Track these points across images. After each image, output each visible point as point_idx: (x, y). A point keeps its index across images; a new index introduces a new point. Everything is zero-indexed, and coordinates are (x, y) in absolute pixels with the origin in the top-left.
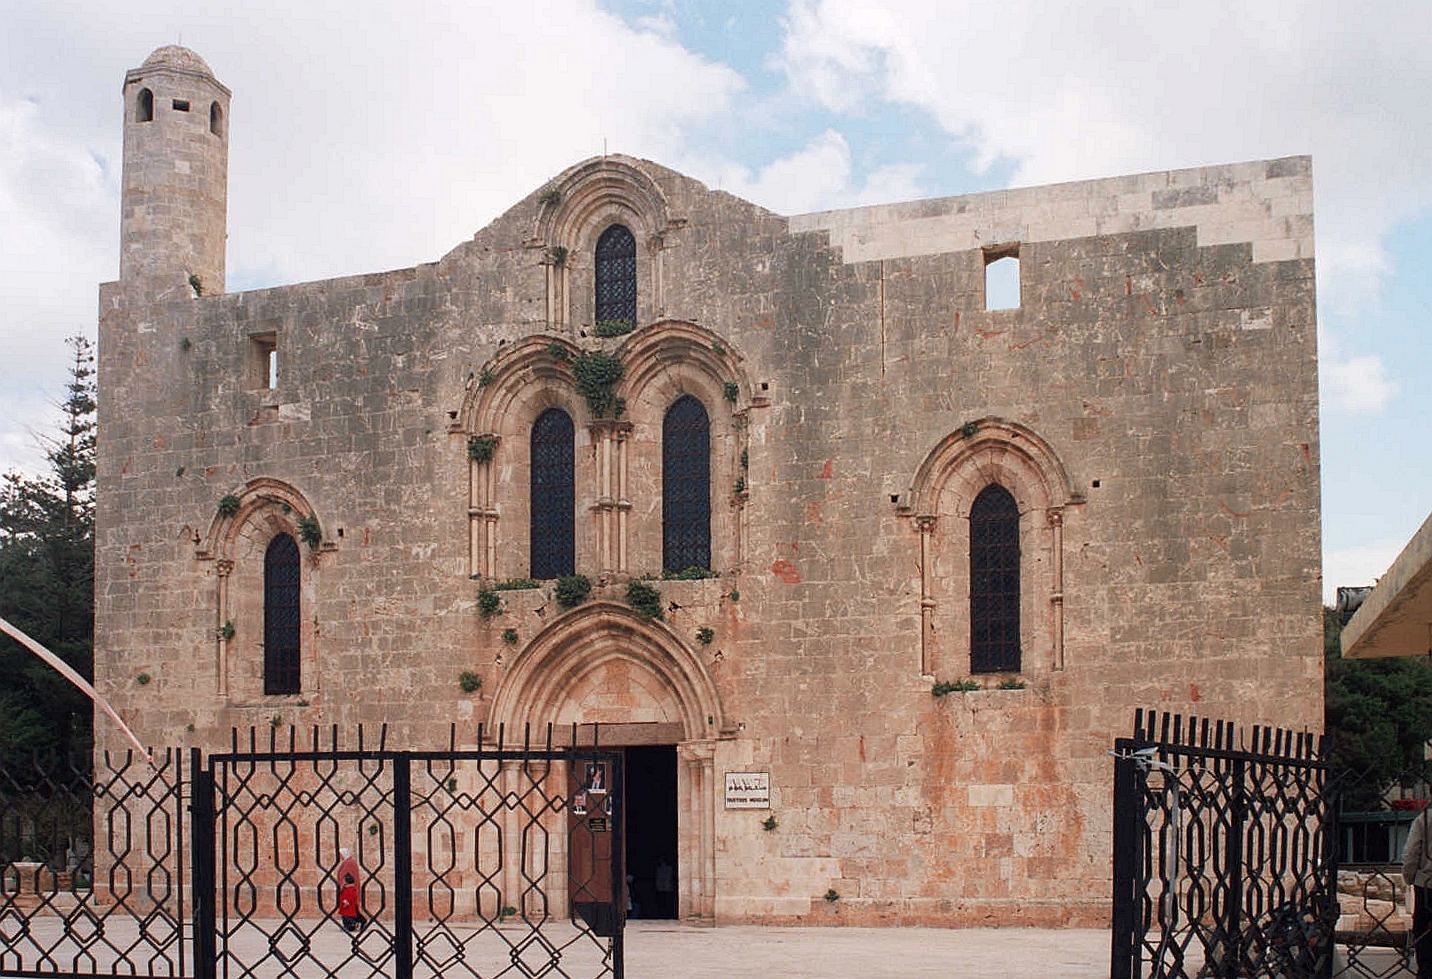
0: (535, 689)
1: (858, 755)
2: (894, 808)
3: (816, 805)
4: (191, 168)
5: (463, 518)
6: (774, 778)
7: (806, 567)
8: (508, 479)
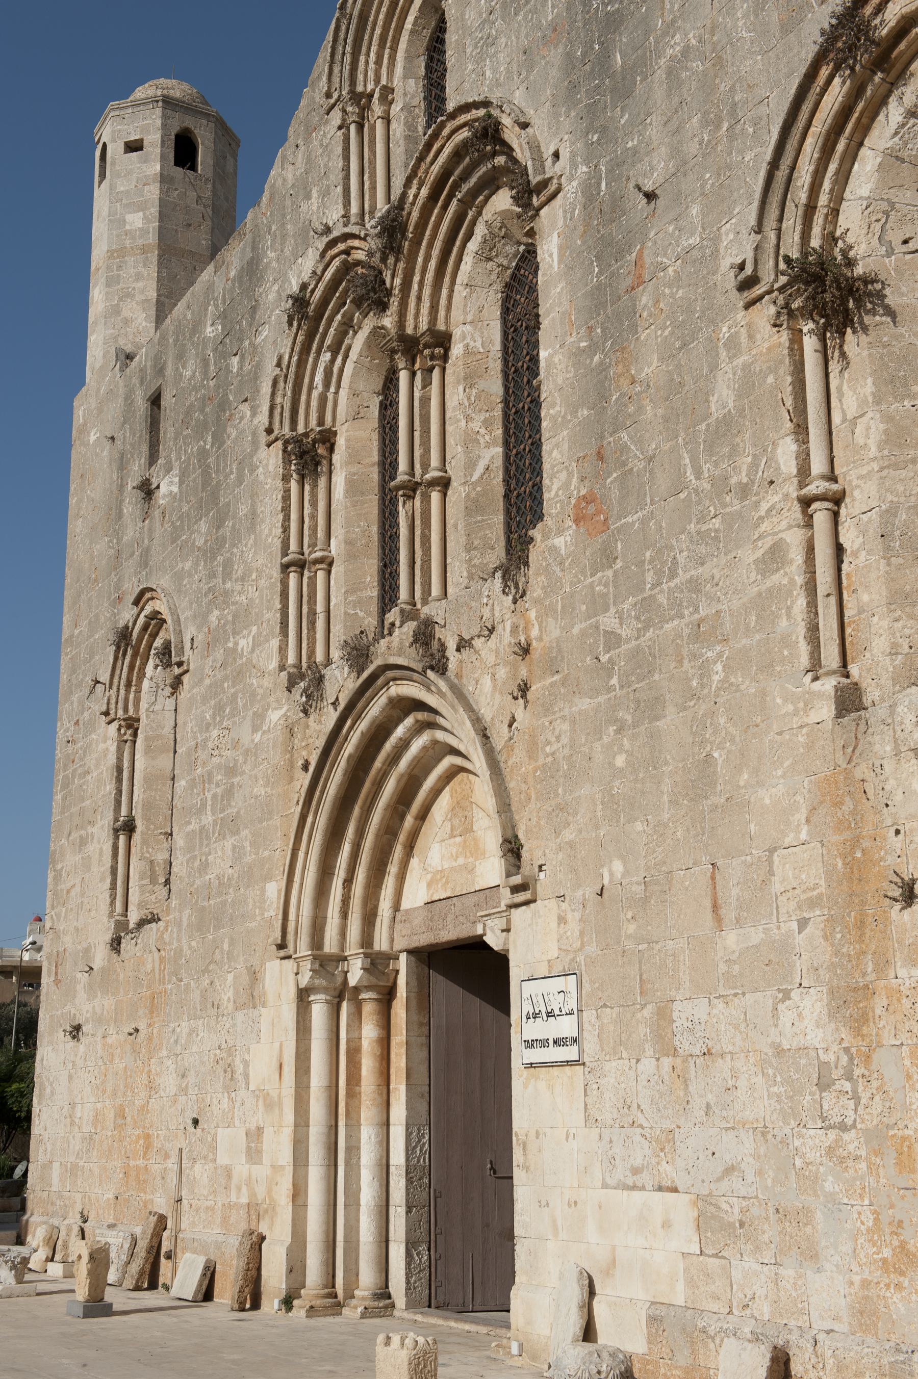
1: (709, 915)
2: (779, 1051)
3: (649, 1052)
4: (145, 217)
5: (276, 574)
6: (586, 986)
7: (615, 493)
8: (341, 495)
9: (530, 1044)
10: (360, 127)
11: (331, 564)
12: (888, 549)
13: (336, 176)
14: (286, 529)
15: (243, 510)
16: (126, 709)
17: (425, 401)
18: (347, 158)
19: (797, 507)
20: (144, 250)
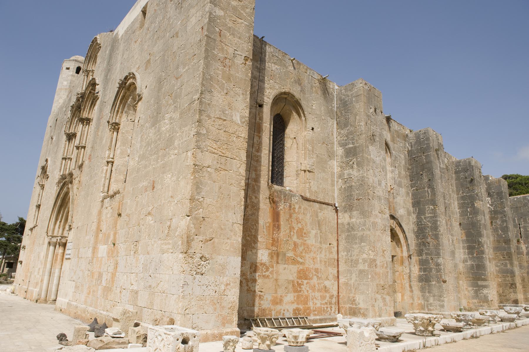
0: (61, 215)
5: (61, 159)
9: (67, 254)
10: (87, 76)
11: (71, 159)
12: (116, 172)
13: (82, 85)
14: (64, 151)
15: (60, 146)
16: (42, 183)
17: (85, 131)
18: (84, 82)
19: (106, 163)
20: (66, 89)
